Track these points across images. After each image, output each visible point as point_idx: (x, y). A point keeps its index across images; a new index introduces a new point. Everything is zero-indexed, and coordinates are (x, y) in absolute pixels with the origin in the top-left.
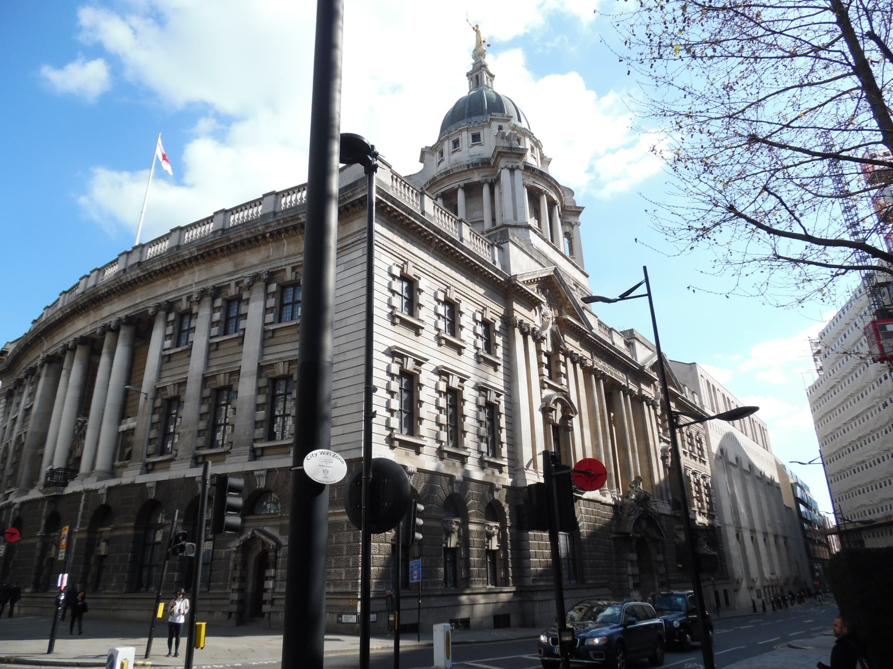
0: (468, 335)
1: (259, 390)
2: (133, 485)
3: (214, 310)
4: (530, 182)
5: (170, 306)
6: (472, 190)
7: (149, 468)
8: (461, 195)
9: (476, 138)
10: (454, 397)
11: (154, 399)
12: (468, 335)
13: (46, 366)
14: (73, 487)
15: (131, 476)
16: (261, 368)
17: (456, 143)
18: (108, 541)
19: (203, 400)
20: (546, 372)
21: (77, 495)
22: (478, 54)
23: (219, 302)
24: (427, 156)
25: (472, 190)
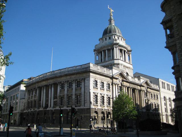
3: (67, 84)
4: (120, 48)
5: (60, 82)
6: (109, 50)
11: (60, 97)
13: (38, 88)
14: (48, 109)
17: (106, 39)
18: (55, 117)
19: (67, 98)
20: (119, 90)
21: (49, 110)
23: (68, 83)
24: (100, 40)
25: (109, 50)
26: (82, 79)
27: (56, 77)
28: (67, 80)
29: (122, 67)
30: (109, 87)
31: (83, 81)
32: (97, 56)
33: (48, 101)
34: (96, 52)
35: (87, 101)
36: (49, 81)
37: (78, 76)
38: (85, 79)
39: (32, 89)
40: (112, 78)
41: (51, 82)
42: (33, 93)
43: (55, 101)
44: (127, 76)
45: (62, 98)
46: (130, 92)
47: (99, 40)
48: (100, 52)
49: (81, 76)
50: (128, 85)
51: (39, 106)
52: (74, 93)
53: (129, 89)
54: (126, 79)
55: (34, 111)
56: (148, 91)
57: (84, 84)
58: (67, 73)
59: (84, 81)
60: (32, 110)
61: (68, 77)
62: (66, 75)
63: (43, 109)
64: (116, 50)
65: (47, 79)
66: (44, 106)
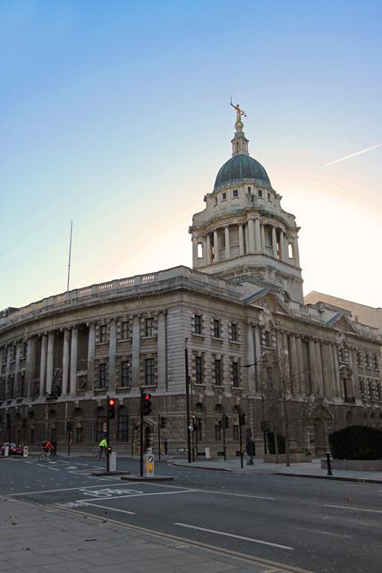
0: (225, 334)
1: (141, 364)
2: (90, 400)
3: (117, 327)
4: (265, 222)
5: (96, 323)
7: (96, 394)
8: (227, 231)
9: (236, 193)
10: (218, 363)
12: (225, 334)
14: (60, 400)
15: (89, 396)
16: (141, 355)
17: (224, 195)
18: (81, 422)
20: (264, 343)
22: (239, 125)
23: (119, 324)
24: (208, 200)
26: (161, 312)
27: (84, 308)
28: (115, 316)
29: (273, 275)
30: (234, 334)
31: (162, 318)
32: (200, 246)
33: (61, 377)
34: (196, 234)
35: (173, 376)
36: (63, 320)
37: (148, 303)
38: (167, 311)
39: (11, 345)
40: (246, 307)
41: (71, 320)
42: (15, 354)
43: (80, 377)
44: (285, 301)
45: (102, 367)
46: (297, 345)
47: (205, 200)
48: (208, 234)
49: (156, 302)
50: (289, 326)
51: (36, 393)
52: (135, 354)
53: (293, 339)
54: (285, 311)
55: (19, 407)
56: (349, 345)
57: (166, 326)
58: (115, 295)
59: (166, 319)
60: (14, 404)
61: (120, 308)
62: (113, 302)
63: (47, 399)
64: (254, 227)
65: (57, 315)
66: (49, 391)
